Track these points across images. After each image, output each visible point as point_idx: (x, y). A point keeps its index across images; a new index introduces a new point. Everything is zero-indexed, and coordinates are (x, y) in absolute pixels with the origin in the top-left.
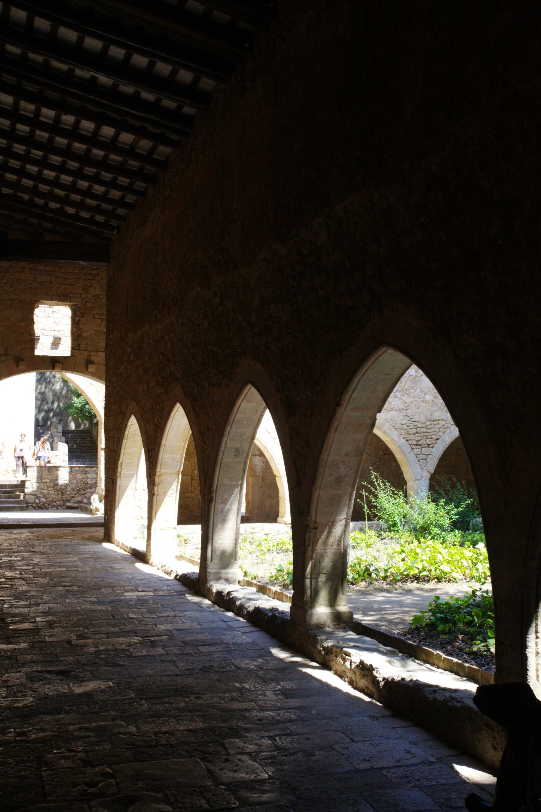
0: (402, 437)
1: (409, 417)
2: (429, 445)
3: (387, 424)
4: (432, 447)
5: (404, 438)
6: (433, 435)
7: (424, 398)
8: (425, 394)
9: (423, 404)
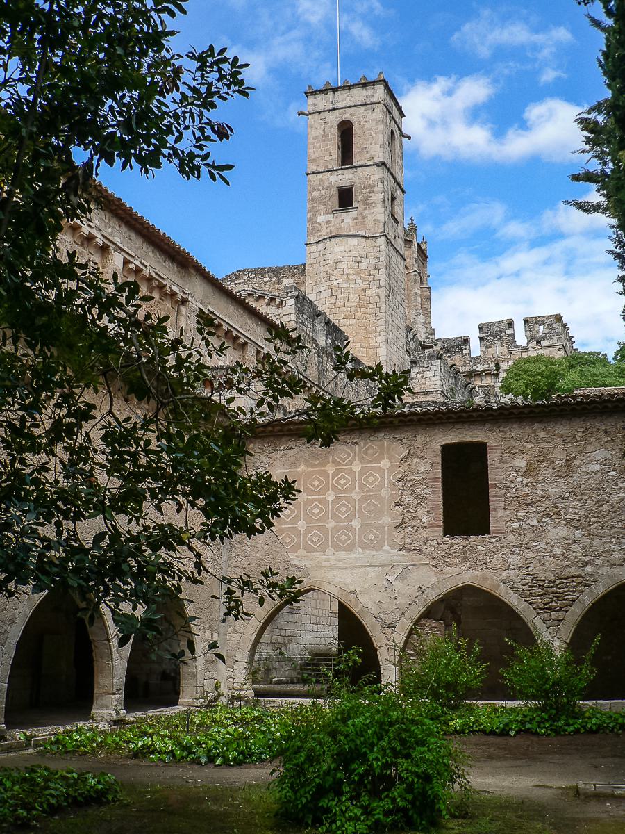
0: (523, 600)
1: (532, 575)
2: (561, 608)
3: (503, 585)
4: (566, 611)
5: (526, 601)
6: (566, 595)
7: (551, 551)
8: (553, 546)
9: (551, 559)
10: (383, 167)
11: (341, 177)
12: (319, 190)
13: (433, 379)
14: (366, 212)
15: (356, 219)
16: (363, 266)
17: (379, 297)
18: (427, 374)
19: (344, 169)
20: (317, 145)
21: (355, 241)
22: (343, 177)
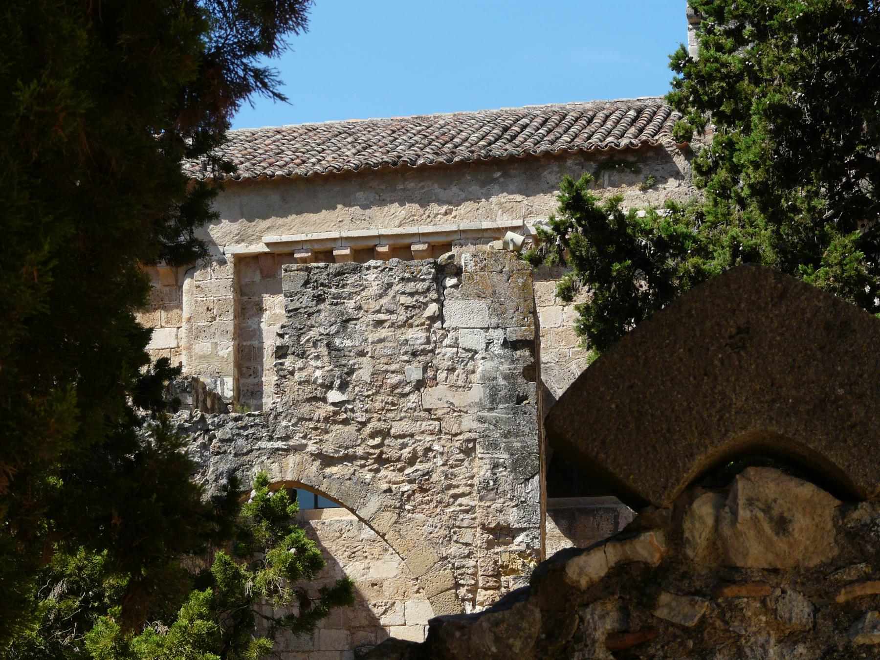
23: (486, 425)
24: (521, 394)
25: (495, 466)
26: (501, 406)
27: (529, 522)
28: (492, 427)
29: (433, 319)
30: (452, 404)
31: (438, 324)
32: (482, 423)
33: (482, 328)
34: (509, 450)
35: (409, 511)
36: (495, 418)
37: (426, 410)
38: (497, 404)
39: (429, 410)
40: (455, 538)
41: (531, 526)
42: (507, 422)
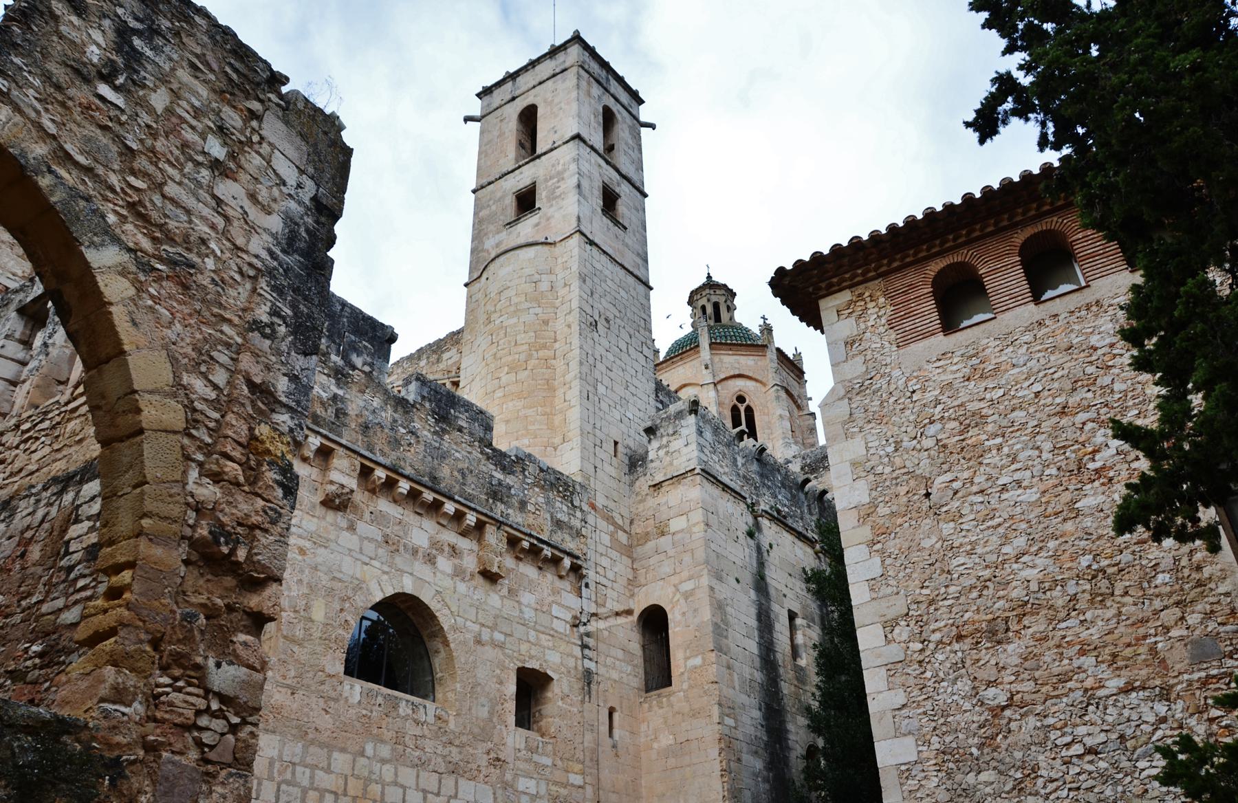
10: (577, 141)
11: (517, 179)
12: (488, 206)
13: (685, 450)
14: (552, 210)
15: (537, 225)
16: (544, 286)
17: (569, 326)
18: (676, 444)
19: (523, 165)
20: (489, 152)
21: (531, 251)
22: (522, 176)
23: (275, 263)
24: (318, 260)
25: (275, 312)
26: (298, 258)
27: (298, 402)
28: (281, 270)
29: (253, 115)
30: (246, 213)
31: (254, 124)
32: (272, 258)
33: (297, 167)
34: (294, 307)
35: (152, 297)
36: (288, 264)
37: (214, 197)
38: (294, 251)
39: (219, 202)
40: (203, 369)
41: (299, 409)
42: (298, 276)
